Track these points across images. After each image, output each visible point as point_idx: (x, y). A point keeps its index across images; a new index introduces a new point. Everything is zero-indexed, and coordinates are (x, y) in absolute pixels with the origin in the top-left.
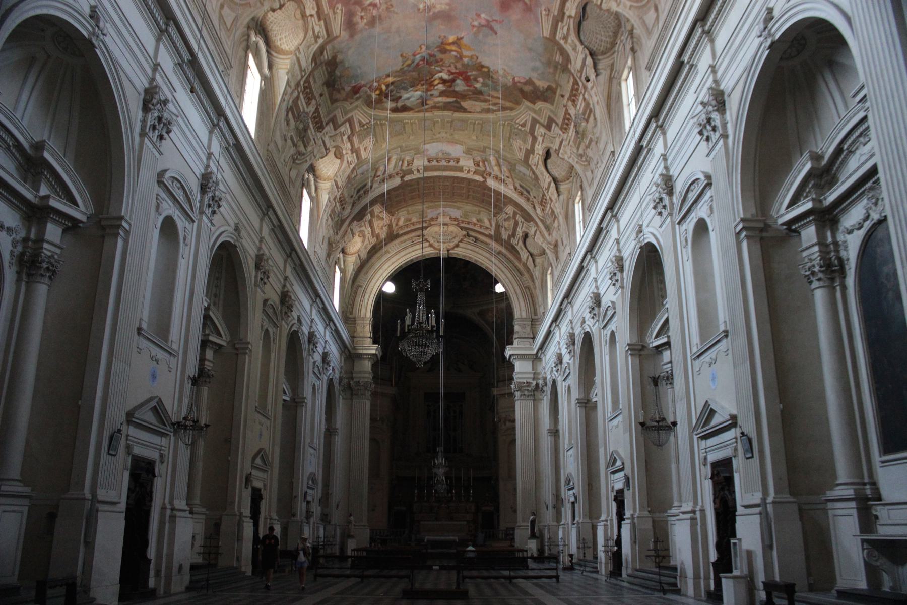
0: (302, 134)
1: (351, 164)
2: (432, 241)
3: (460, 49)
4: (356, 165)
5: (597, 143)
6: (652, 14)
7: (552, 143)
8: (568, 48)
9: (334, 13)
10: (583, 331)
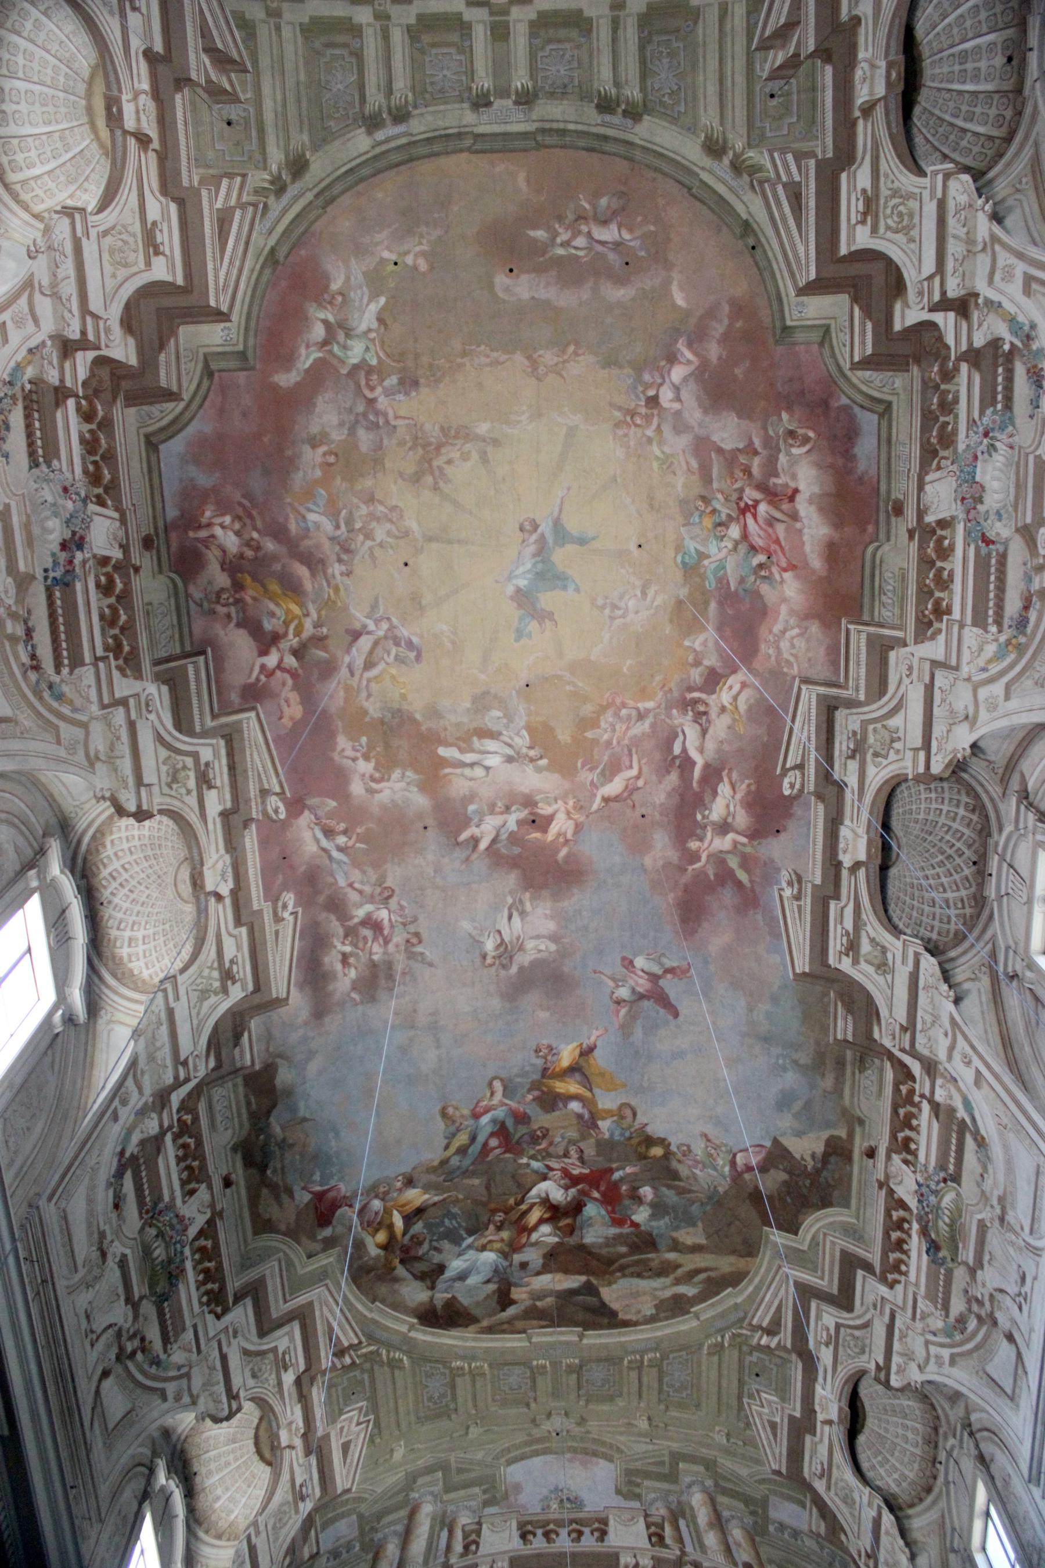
1: (303, 1499)
3: (591, 1090)
4: (316, 1510)
5: (1002, 1220)
7: (863, 1352)
8: (864, 974)
9: (278, 919)
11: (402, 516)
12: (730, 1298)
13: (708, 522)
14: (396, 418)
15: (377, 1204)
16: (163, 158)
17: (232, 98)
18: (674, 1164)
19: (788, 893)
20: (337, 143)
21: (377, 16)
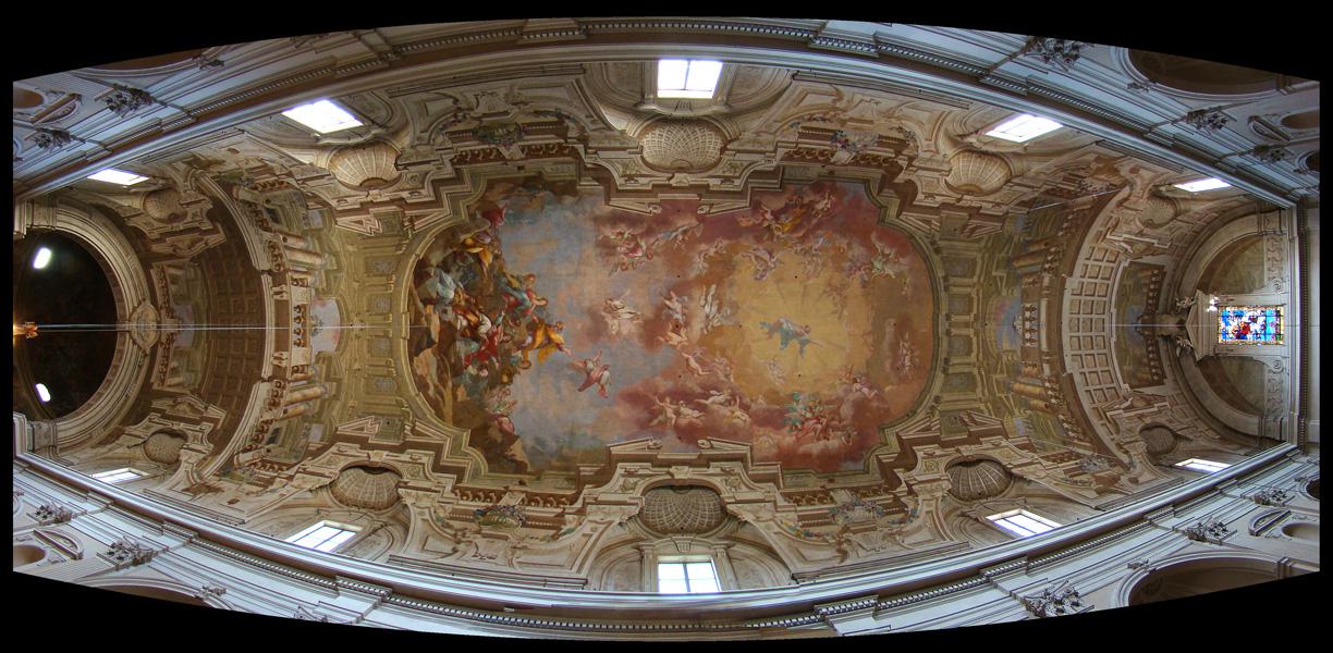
8: (617, 479)
9: (650, 204)
12: (430, 413)
13: (811, 404)
15: (488, 240)
18: (498, 388)
19: (651, 443)
21: (974, 284)
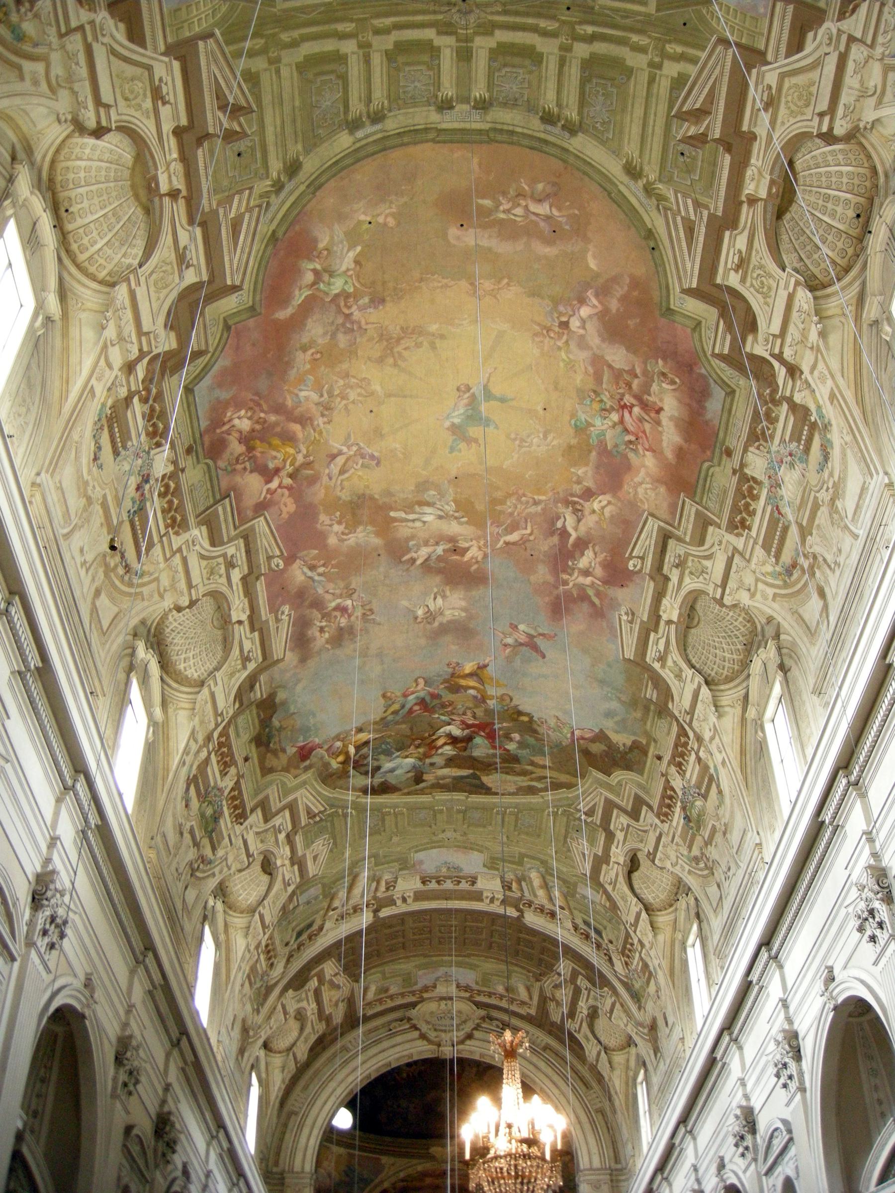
0: (210, 825)
2: (424, 1028)
4: (297, 888)
5: (725, 833)
6: (815, 603)
7: (641, 841)
8: (667, 675)
9: (278, 620)
10: (721, 1185)
11: (369, 384)
12: (563, 793)
13: (596, 406)
14: (367, 324)
15: (339, 744)
16: (189, 200)
17: (243, 135)
18: (535, 726)
20: (326, 144)
21: (360, 46)
